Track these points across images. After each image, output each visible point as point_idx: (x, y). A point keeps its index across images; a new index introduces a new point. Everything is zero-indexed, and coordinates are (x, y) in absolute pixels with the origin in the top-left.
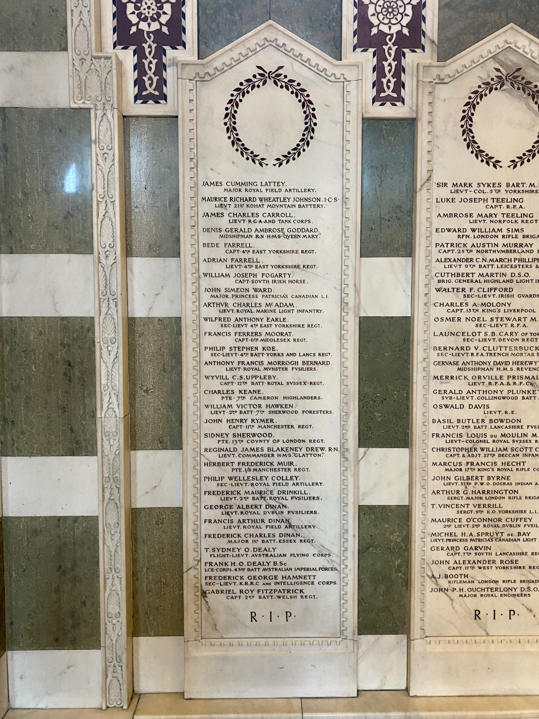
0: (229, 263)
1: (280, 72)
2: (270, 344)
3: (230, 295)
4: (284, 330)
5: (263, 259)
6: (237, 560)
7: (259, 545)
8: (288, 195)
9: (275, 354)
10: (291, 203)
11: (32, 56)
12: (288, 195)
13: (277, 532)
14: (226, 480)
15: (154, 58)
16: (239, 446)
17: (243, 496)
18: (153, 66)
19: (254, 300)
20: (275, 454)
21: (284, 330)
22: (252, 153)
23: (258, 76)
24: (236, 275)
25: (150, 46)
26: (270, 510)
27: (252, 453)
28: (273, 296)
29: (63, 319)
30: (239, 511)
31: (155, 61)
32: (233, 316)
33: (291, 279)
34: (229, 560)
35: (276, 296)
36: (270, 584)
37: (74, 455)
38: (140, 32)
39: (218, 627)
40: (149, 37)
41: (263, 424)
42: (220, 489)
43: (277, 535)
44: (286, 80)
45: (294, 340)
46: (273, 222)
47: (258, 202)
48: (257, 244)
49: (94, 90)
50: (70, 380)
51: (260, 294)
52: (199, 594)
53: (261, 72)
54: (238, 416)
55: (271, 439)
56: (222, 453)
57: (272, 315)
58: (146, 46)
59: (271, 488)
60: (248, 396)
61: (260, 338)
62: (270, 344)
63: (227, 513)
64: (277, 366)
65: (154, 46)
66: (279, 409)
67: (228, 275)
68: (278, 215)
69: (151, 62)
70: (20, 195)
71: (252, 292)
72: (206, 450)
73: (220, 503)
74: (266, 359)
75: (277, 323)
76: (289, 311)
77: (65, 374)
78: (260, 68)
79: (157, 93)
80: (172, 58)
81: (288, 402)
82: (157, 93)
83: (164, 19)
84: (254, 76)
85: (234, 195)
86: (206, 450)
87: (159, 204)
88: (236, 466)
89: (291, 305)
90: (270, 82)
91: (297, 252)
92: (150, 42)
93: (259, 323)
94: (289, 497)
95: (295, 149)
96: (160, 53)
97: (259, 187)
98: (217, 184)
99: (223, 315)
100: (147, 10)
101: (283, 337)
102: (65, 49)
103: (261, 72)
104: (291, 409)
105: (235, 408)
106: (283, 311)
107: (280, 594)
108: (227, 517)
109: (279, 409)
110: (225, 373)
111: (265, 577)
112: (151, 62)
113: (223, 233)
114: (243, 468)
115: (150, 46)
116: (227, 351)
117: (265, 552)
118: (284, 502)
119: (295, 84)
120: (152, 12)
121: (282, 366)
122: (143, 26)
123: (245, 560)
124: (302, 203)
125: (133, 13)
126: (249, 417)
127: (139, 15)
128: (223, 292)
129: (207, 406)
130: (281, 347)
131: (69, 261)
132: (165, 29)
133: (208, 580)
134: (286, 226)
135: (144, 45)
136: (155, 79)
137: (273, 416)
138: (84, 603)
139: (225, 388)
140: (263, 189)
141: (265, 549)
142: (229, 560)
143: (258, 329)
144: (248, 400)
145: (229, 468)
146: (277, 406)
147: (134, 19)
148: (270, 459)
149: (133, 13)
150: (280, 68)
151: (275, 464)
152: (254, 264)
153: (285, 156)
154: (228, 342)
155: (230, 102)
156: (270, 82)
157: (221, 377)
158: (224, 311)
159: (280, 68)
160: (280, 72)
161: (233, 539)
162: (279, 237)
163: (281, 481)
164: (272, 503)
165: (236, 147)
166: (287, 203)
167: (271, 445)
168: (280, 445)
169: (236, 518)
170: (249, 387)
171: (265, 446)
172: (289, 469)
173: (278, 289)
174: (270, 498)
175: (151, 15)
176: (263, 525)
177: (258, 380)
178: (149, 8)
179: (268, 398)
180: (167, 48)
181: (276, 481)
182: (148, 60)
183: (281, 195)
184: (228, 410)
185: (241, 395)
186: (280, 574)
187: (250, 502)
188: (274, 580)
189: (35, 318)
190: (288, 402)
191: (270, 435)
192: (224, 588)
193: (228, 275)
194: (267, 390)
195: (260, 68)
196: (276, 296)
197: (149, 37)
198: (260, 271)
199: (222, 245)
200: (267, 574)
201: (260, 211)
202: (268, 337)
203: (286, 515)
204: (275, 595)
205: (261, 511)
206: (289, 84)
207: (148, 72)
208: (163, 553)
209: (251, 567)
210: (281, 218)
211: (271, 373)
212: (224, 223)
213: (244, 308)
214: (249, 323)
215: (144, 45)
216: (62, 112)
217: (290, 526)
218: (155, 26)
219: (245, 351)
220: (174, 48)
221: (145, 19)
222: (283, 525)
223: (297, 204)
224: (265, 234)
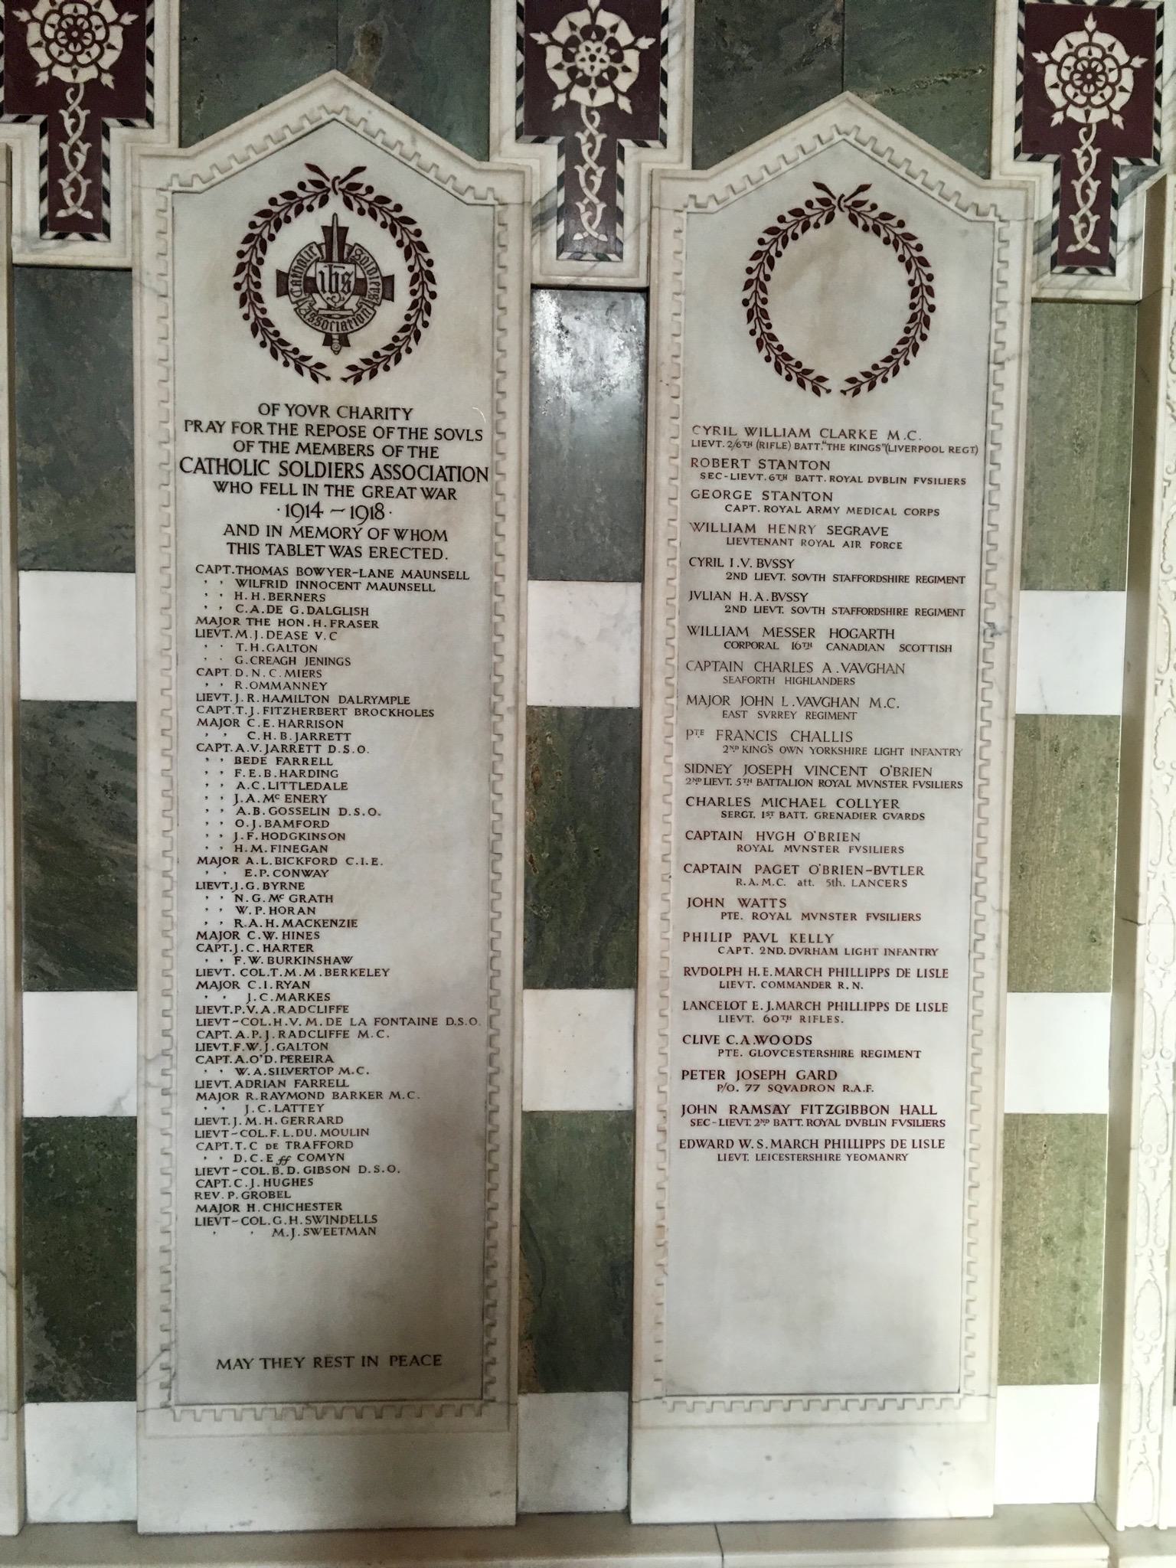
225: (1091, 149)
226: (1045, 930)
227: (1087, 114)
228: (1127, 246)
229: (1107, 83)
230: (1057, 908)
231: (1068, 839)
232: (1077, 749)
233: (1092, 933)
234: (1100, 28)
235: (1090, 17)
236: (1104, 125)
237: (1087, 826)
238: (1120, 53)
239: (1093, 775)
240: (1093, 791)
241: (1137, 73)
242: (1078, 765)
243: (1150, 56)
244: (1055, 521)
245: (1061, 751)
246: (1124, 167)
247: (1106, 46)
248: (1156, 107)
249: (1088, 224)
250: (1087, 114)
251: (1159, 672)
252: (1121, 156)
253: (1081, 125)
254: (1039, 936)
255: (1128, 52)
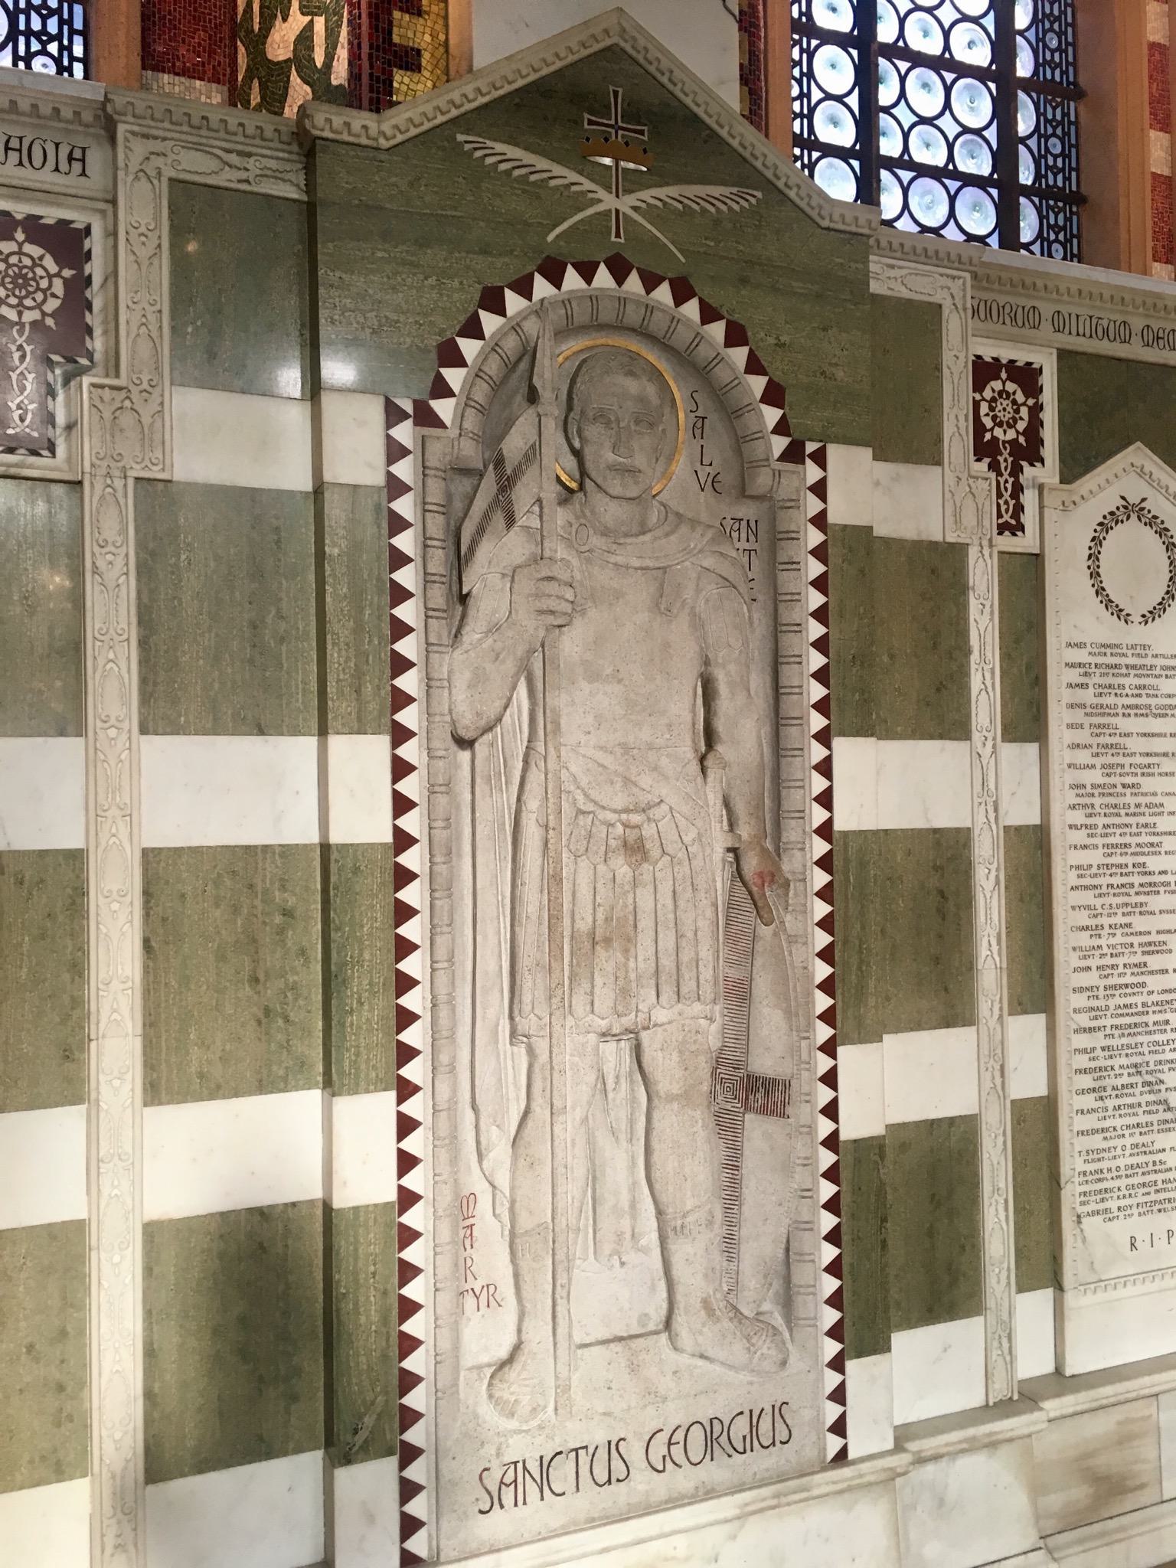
0: (1095, 750)
1: (1143, 505)
2: (1141, 859)
3: (1096, 792)
4: (1155, 839)
5: (1135, 744)
6: (1113, 1164)
7: (1138, 1139)
8: (1155, 662)
9: (1146, 873)
10: (1157, 672)
11: (902, 469)
12: (1155, 662)
13: (1154, 1118)
14: (1099, 1052)
15: (1010, 475)
16: (1112, 1003)
17: (1117, 1072)
18: (1009, 486)
19: (1121, 801)
20: (1150, 1010)
21: (1155, 839)
22: (1117, 606)
23: (1122, 509)
24: (1103, 767)
25: (1006, 460)
26: (1147, 1089)
27: (1125, 1011)
28: (1142, 794)
29: (935, 831)
30: (1114, 1093)
31: (1011, 480)
32: (1100, 821)
33: (1160, 771)
34: (1104, 1165)
35: (1146, 794)
36: (1148, 1194)
37: (948, 1026)
38: (994, 439)
39: (1095, 1266)
40: (1005, 448)
41: (1136, 970)
42: (1093, 1064)
43: (1155, 1123)
44: (1150, 516)
45: (1166, 853)
46: (1139, 696)
47: (1124, 671)
48: (1125, 724)
49: (969, 519)
50: (944, 919)
51: (1128, 791)
52: (1075, 1218)
53: (1124, 503)
54: (1108, 961)
55: (1145, 990)
56: (1093, 1014)
57: (1142, 820)
58: (1001, 459)
59: (1147, 1058)
60: (1119, 932)
61: (1129, 851)
62: (1141, 859)
63: (1101, 1098)
64: (1149, 889)
65: (1010, 460)
66: (1152, 948)
67: (1093, 767)
68: (1145, 687)
69: (1006, 481)
70: (885, 658)
71: (1120, 789)
72: (1075, 1011)
73: (1092, 1084)
74: (1137, 880)
75: (1147, 830)
76: (1159, 814)
77: (938, 910)
78: (1123, 498)
79: (1013, 522)
80: (1030, 477)
81: (1162, 937)
82: (1013, 522)
83: (1021, 426)
84: (1118, 508)
85: (1100, 660)
86: (1075, 1011)
87: (1015, 670)
88: (1108, 1031)
89: (1162, 805)
90: (1134, 517)
91: (1165, 736)
92: (1006, 454)
93: (1127, 830)
94: (1166, 1068)
95: (1160, 604)
96: (1016, 471)
97: (1124, 651)
98: (1081, 645)
99: (1089, 821)
100: (1002, 413)
101: (1153, 849)
102: (939, 463)
103: (1124, 503)
104: (1164, 948)
105: (1105, 950)
106: (1154, 814)
107: (1161, 1207)
108: (1100, 1104)
109: (1152, 948)
110: (1092, 901)
111: (1144, 1185)
112: (1006, 481)
113: (1089, 710)
114: (1116, 1033)
115: (1006, 460)
116: (1094, 870)
117: (1144, 1149)
118: (1160, 1076)
119: (1159, 521)
120: (1008, 416)
121: (1152, 889)
122: (998, 432)
123: (1121, 1162)
124: (1169, 673)
125: (987, 415)
126: (1120, 961)
127: (994, 418)
128: (1089, 789)
129: (1074, 949)
130: (1153, 863)
131: (943, 749)
132: (1022, 439)
133: (1083, 1198)
134: (1153, 701)
135: (999, 457)
136: (1012, 503)
137: (1146, 958)
138: (963, 1247)
139: (1092, 922)
140: (1130, 653)
141: (1143, 1145)
142: (1104, 1165)
143: (1127, 839)
144: (1119, 939)
145: (1101, 1034)
146: (1150, 944)
147: (988, 422)
148: (1145, 1019)
149: (987, 415)
150: (1144, 500)
151: (1151, 1024)
152: (1121, 751)
153: (1151, 612)
154: (1095, 857)
155: (1093, 539)
156: (1134, 517)
157: (1088, 907)
158: (1090, 815)
159: (1144, 500)
160: (1143, 505)
161: (1108, 1135)
162: (1147, 716)
163: (1157, 1048)
164: (1149, 1078)
165: (1100, 598)
166: (1154, 672)
167: (1144, 998)
168: (1155, 998)
169: (1110, 1103)
170: (1120, 920)
171: (1138, 1000)
172: (1165, 1031)
173: (1148, 784)
174: (1147, 1072)
175: (1006, 419)
176: (1140, 1111)
177: (1129, 909)
178: (1004, 409)
179: (1141, 933)
180: (1024, 463)
181: (1153, 1048)
182: (1004, 478)
183: (1148, 661)
184: (1097, 953)
185: (1112, 931)
186: (1160, 1177)
187: (1125, 1080)
188: (1154, 1188)
189: (902, 830)
190: (1162, 937)
191: (1143, 985)
192: (1101, 1206)
193: (1093, 767)
194: (1140, 923)
195: (1123, 498)
196: (1146, 794)
197: (1005, 448)
198: (1127, 761)
199: (1086, 726)
200: (1148, 1179)
201: (1126, 681)
202: (1138, 850)
203: (1163, 1095)
204: (1155, 1208)
205: (1137, 1091)
206: (1152, 522)
207: (1004, 493)
208: (1026, 1166)
209: (1129, 1172)
210: (1148, 691)
211: (1142, 899)
212: (1088, 696)
213: (1112, 810)
214: (1118, 831)
215: (999, 457)
216: (933, 545)
217: (1169, 1109)
218: (1011, 435)
219: (1114, 870)
220: (1032, 465)
221: (1000, 425)
222: (1161, 1108)
223: (1164, 673)
224: (1132, 712)
225: (25, 345)
226: (17, 1053)
227: (20, 314)
228: (65, 434)
229: (38, 289)
230: (28, 1030)
231: (37, 965)
232: (42, 881)
233: (65, 1050)
234: (30, 239)
235: (19, 230)
236: (34, 324)
237: (55, 952)
238: (50, 263)
239: (60, 904)
240: (61, 918)
241: (66, 282)
242: (44, 896)
243: (81, 270)
244: (8, 674)
245: (26, 885)
246: (58, 363)
247: (36, 256)
248: (87, 313)
249: (26, 411)
250: (20, 314)
251: (122, 809)
252: (55, 353)
253: (13, 324)
254: (10, 1059)
255: (57, 262)
